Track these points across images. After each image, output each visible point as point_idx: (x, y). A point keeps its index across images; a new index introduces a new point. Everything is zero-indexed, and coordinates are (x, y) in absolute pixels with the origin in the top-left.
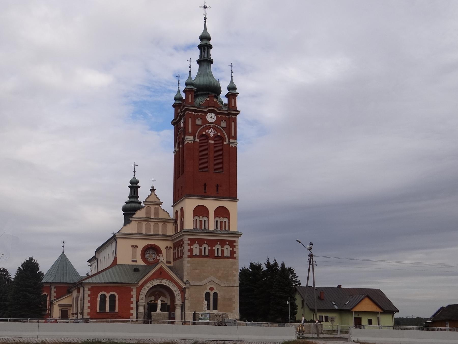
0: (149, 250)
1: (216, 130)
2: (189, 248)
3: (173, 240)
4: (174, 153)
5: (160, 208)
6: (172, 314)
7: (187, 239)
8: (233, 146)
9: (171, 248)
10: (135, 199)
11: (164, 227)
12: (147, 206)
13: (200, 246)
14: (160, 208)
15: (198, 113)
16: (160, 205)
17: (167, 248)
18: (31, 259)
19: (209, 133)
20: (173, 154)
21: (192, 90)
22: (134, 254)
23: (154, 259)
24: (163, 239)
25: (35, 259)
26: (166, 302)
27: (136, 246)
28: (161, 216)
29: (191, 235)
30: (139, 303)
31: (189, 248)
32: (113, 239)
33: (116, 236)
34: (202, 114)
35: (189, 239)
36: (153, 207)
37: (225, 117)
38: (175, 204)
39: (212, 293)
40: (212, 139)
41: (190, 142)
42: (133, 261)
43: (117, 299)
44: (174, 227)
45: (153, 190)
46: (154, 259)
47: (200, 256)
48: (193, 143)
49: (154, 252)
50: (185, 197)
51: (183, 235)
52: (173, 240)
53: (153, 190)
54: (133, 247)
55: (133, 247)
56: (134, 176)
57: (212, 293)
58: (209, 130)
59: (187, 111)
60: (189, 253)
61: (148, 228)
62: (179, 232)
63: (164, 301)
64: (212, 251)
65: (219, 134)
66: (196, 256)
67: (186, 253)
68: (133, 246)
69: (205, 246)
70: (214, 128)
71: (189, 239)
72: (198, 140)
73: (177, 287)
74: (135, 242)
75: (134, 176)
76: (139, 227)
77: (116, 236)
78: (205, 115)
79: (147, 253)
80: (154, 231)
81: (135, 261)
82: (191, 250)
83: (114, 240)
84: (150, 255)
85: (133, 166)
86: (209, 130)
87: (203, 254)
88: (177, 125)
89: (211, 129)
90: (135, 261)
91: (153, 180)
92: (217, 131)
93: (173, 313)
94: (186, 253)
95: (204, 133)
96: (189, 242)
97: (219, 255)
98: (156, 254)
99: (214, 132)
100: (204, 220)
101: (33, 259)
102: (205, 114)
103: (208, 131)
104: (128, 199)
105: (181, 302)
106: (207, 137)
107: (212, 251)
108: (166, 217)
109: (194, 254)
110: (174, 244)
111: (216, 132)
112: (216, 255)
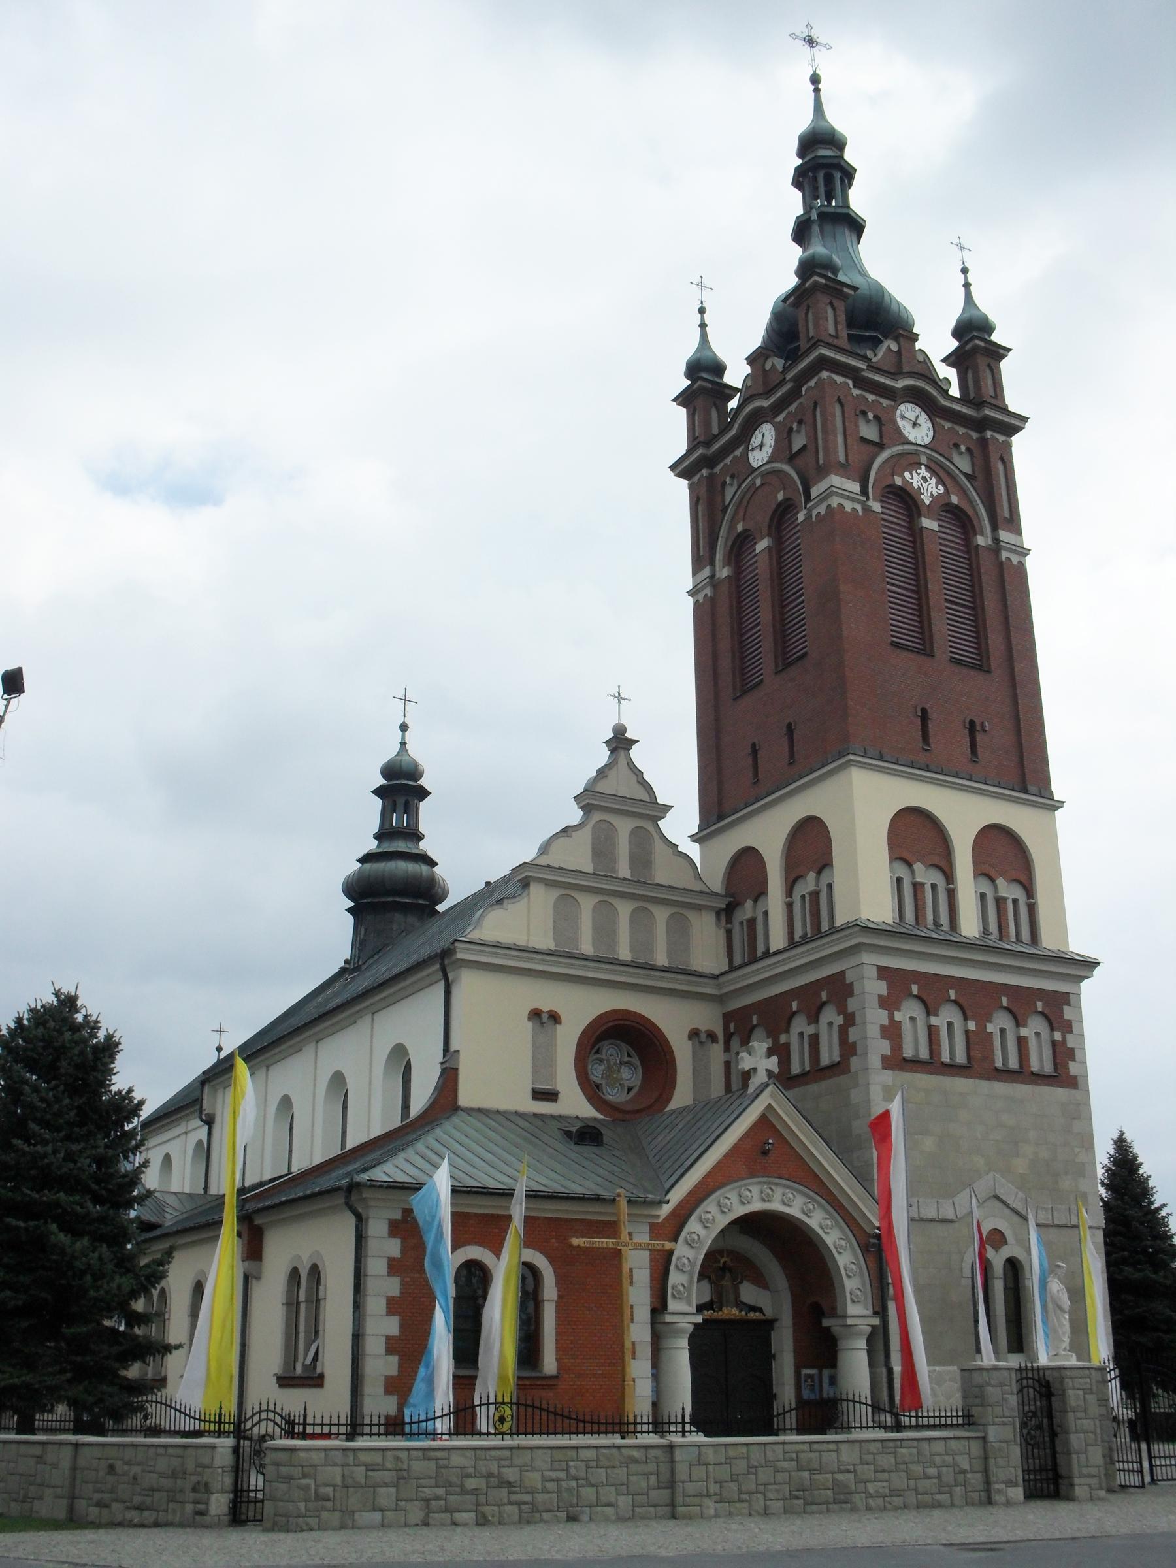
0: (606, 1042)
1: (940, 481)
2: (882, 1017)
3: (720, 999)
4: (691, 593)
5: (656, 837)
6: (803, 1379)
7: (873, 972)
8: (1015, 559)
9: (712, 1036)
10: (410, 845)
11: (679, 930)
12: (597, 816)
13: (929, 1011)
14: (656, 837)
15: (864, 393)
16: (655, 820)
17: (694, 1034)
18: (69, 1002)
19: (916, 487)
20: (690, 602)
21: (838, 287)
22: (542, 1059)
23: (630, 1090)
24: (677, 987)
25: (91, 1004)
26: (769, 1313)
27: (555, 1018)
28: (662, 875)
29: (897, 949)
30: (668, 1318)
31: (882, 1017)
32: (437, 966)
33: (460, 955)
34: (882, 400)
35: (884, 972)
36: (624, 827)
37: (967, 433)
38: (708, 831)
39: (998, 1260)
40: (930, 511)
41: (848, 506)
42: (540, 1095)
43: (550, 1290)
44: (722, 935)
45: (620, 743)
46: (630, 1090)
47: (933, 1065)
48: (860, 513)
49: (629, 1055)
50: (851, 757)
51: (856, 949)
52: (720, 999)
53: (620, 743)
54: (544, 1019)
55: (544, 1019)
56: (403, 744)
57: (998, 1260)
58: (914, 472)
59: (827, 370)
60: (885, 1047)
61: (605, 930)
62: (777, 953)
63: (760, 1310)
64: (977, 1042)
65: (954, 499)
66: (914, 1064)
67: (879, 1048)
68: (535, 1014)
69: (947, 1015)
70: (934, 471)
71: (884, 972)
72: (876, 507)
73: (847, 1230)
74: (548, 997)
75: (403, 744)
76: (564, 917)
77: (460, 955)
78: (891, 406)
79: (598, 1056)
80: (632, 949)
81: (549, 1096)
82: (892, 1032)
83: (440, 975)
84: (609, 1068)
85: (401, 704)
86: (914, 472)
87: (946, 1058)
88: (709, 471)
89: (923, 471)
90: (549, 1096)
91: (619, 697)
92: (944, 485)
93: (811, 1376)
94: (879, 1048)
95: (898, 481)
96: (881, 987)
97: (1011, 1066)
98: (638, 1064)
99: (934, 485)
100: (932, 884)
101: (79, 1003)
102: (893, 403)
103: (912, 479)
104: (372, 845)
105: (869, 1312)
106: (906, 499)
107: (977, 1042)
108: (684, 880)
109: (908, 1053)
110: (727, 1017)
111: (941, 489)
112: (999, 1064)
